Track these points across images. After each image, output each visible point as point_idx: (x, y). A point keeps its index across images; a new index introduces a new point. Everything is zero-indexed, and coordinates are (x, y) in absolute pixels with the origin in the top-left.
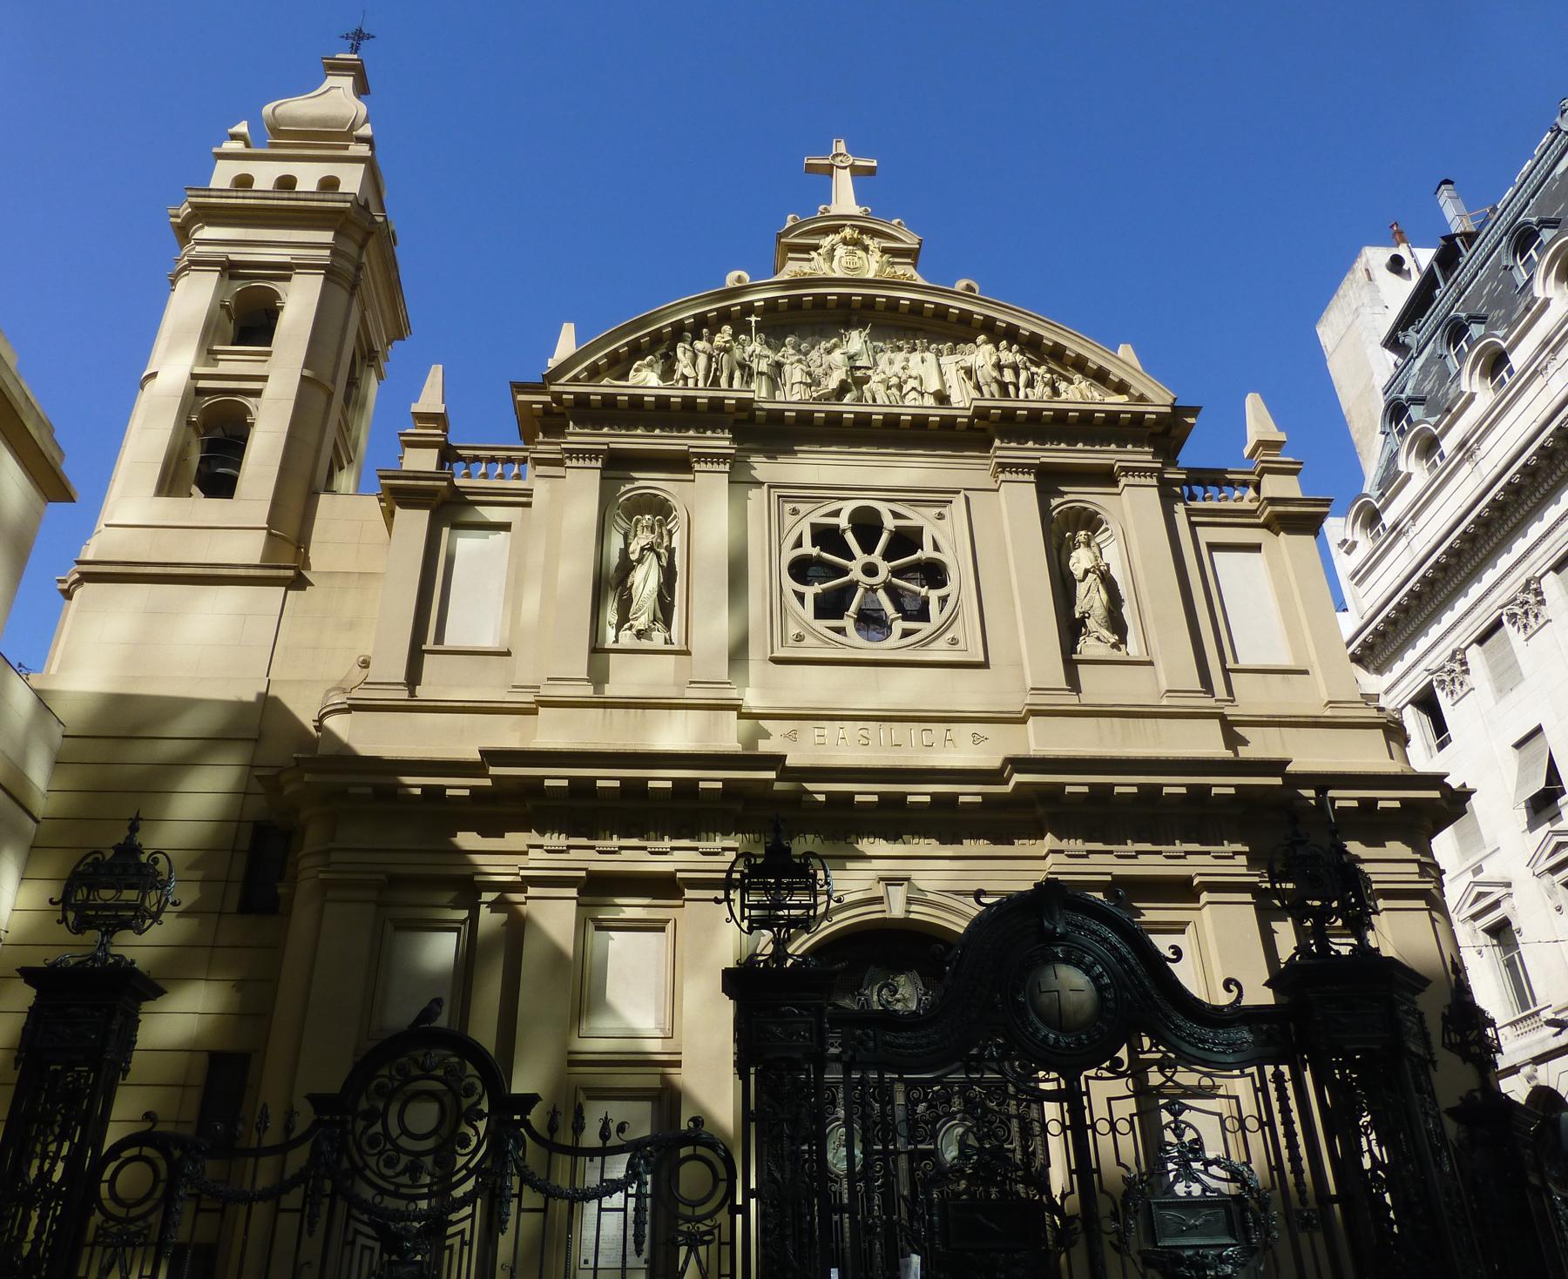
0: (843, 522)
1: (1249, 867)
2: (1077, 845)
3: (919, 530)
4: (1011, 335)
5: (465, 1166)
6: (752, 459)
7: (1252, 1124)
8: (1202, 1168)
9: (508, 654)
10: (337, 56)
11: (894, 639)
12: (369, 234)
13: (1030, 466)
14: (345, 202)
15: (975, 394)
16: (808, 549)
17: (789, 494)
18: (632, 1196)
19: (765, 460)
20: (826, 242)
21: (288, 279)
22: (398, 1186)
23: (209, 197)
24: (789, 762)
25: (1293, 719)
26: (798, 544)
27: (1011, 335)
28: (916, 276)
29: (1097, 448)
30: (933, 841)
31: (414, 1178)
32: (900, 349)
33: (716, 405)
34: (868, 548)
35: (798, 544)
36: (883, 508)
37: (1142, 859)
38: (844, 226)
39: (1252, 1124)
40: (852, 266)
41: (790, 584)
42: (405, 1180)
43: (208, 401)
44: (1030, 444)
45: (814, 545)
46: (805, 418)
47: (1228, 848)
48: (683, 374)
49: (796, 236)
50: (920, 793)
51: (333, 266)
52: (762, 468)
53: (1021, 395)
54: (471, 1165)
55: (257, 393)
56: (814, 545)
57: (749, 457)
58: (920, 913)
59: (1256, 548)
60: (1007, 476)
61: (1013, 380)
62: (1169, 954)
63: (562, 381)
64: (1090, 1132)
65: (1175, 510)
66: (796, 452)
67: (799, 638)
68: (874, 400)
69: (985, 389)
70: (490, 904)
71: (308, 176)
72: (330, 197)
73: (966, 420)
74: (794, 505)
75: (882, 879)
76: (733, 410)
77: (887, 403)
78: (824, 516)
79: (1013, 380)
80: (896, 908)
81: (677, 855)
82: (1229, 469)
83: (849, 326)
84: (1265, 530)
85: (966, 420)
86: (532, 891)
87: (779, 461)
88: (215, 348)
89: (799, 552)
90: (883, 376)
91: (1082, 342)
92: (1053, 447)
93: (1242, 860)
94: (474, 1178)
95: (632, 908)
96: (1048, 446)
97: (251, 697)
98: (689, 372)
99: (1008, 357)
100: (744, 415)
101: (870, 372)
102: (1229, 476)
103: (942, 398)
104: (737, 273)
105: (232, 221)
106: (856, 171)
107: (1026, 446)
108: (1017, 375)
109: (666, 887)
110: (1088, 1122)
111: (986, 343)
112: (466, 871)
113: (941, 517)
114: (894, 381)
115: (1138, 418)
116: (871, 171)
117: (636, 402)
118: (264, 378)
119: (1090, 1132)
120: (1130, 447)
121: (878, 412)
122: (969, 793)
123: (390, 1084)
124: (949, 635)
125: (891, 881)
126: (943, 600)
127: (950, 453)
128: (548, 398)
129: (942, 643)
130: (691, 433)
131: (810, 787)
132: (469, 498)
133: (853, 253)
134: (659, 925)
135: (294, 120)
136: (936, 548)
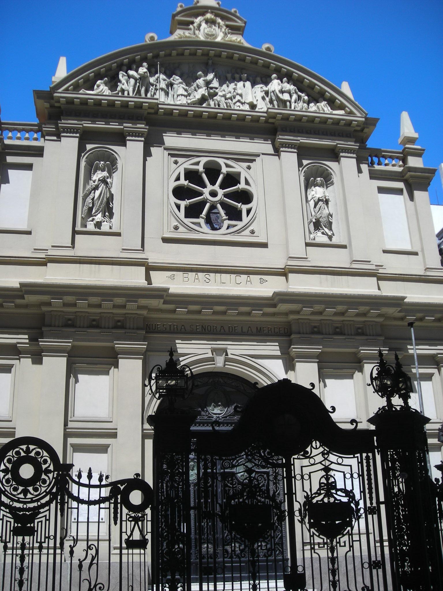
3: (239, 174)
5: (45, 491)
7: (355, 475)
8: (335, 492)
11: (223, 230)
15: (270, 106)
16: (183, 181)
18: (112, 503)
20: (198, 20)
22: (19, 498)
24: (170, 291)
26: (178, 179)
28: (243, 41)
31: (25, 495)
33: (139, 106)
34: (213, 183)
39: (355, 475)
40: (210, 33)
42: (22, 496)
45: (186, 180)
48: (122, 88)
53: (293, 108)
54: (47, 491)
56: (186, 180)
61: (289, 99)
62: (330, 410)
63: (60, 90)
64: (293, 479)
67: (176, 228)
68: (219, 105)
76: (147, 108)
77: (226, 107)
79: (289, 99)
80: (220, 362)
89: (178, 183)
90: (224, 93)
94: (49, 495)
98: (125, 87)
99: (288, 87)
100: (152, 111)
103: (253, 106)
104: (151, 34)
108: (291, 96)
110: (293, 475)
113: (249, 168)
114: (228, 96)
115: (349, 123)
117: (98, 103)
119: (293, 479)
123: (13, 459)
124: (251, 228)
126: (249, 211)
129: (247, 232)
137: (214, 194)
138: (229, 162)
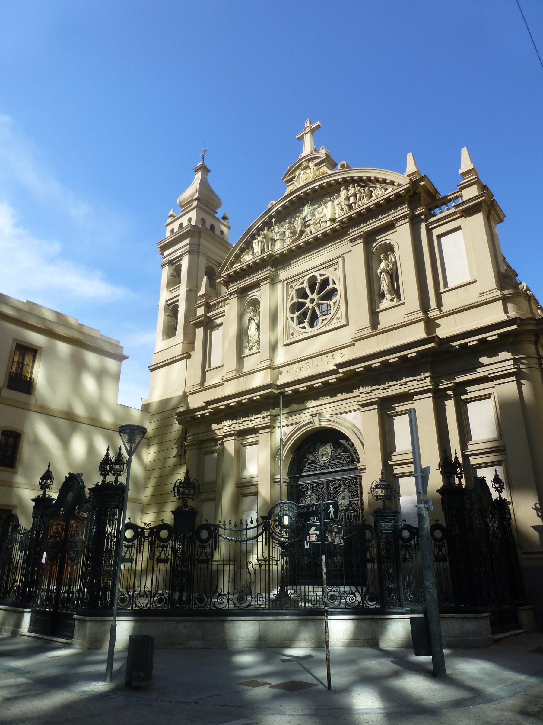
0: (305, 285)
1: (431, 382)
2: (368, 389)
4: (346, 183)
6: (279, 273)
9: (222, 366)
10: (197, 166)
12: (200, 232)
13: (360, 236)
14: (188, 228)
16: (295, 300)
17: (289, 282)
19: (283, 271)
20: (297, 173)
21: (181, 260)
23: (162, 243)
25: (459, 309)
26: (292, 299)
27: (353, 181)
29: (387, 215)
30: (328, 397)
32: (322, 205)
35: (292, 299)
36: (317, 274)
37: (391, 388)
38: (303, 162)
41: (290, 315)
43: (171, 306)
44: (362, 226)
46: (290, 251)
47: (423, 376)
49: (289, 176)
50: (317, 383)
51: (191, 250)
52: (283, 274)
55: (178, 300)
57: (278, 272)
58: (324, 424)
59: (459, 228)
60: (354, 244)
63: (223, 272)
65: (421, 227)
66: (290, 265)
67: (292, 334)
68: (311, 232)
69: (344, 210)
70: (220, 444)
71: (184, 220)
72: (182, 230)
73: (339, 226)
74: (291, 285)
75: (311, 415)
78: (299, 285)
81: (257, 420)
82: (448, 195)
83: (304, 205)
84: (463, 218)
85: (339, 226)
86: (225, 439)
87: (287, 269)
88: (171, 289)
91: (375, 171)
92: (371, 222)
93: (429, 379)
95: (250, 439)
96: (368, 223)
97: (181, 394)
101: (310, 222)
102: (448, 198)
105: (170, 246)
106: (312, 131)
107: (361, 227)
109: (253, 431)
111: (344, 189)
112: (213, 436)
113: (335, 269)
115: (398, 195)
116: (318, 127)
118: (178, 295)
120: (399, 208)
121: (319, 234)
122: (332, 379)
124: (336, 317)
125: (313, 415)
127: (339, 241)
128: (222, 279)
129: (335, 321)
130: (260, 272)
131: (287, 389)
132: (212, 318)
133: (304, 173)
134: (257, 442)
135: (184, 200)
136: (334, 283)
137: (312, 301)
138: (321, 272)
